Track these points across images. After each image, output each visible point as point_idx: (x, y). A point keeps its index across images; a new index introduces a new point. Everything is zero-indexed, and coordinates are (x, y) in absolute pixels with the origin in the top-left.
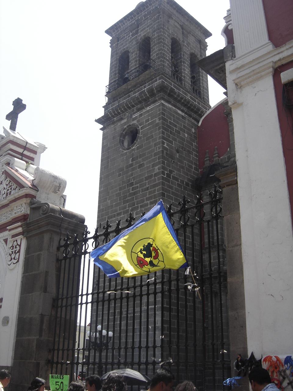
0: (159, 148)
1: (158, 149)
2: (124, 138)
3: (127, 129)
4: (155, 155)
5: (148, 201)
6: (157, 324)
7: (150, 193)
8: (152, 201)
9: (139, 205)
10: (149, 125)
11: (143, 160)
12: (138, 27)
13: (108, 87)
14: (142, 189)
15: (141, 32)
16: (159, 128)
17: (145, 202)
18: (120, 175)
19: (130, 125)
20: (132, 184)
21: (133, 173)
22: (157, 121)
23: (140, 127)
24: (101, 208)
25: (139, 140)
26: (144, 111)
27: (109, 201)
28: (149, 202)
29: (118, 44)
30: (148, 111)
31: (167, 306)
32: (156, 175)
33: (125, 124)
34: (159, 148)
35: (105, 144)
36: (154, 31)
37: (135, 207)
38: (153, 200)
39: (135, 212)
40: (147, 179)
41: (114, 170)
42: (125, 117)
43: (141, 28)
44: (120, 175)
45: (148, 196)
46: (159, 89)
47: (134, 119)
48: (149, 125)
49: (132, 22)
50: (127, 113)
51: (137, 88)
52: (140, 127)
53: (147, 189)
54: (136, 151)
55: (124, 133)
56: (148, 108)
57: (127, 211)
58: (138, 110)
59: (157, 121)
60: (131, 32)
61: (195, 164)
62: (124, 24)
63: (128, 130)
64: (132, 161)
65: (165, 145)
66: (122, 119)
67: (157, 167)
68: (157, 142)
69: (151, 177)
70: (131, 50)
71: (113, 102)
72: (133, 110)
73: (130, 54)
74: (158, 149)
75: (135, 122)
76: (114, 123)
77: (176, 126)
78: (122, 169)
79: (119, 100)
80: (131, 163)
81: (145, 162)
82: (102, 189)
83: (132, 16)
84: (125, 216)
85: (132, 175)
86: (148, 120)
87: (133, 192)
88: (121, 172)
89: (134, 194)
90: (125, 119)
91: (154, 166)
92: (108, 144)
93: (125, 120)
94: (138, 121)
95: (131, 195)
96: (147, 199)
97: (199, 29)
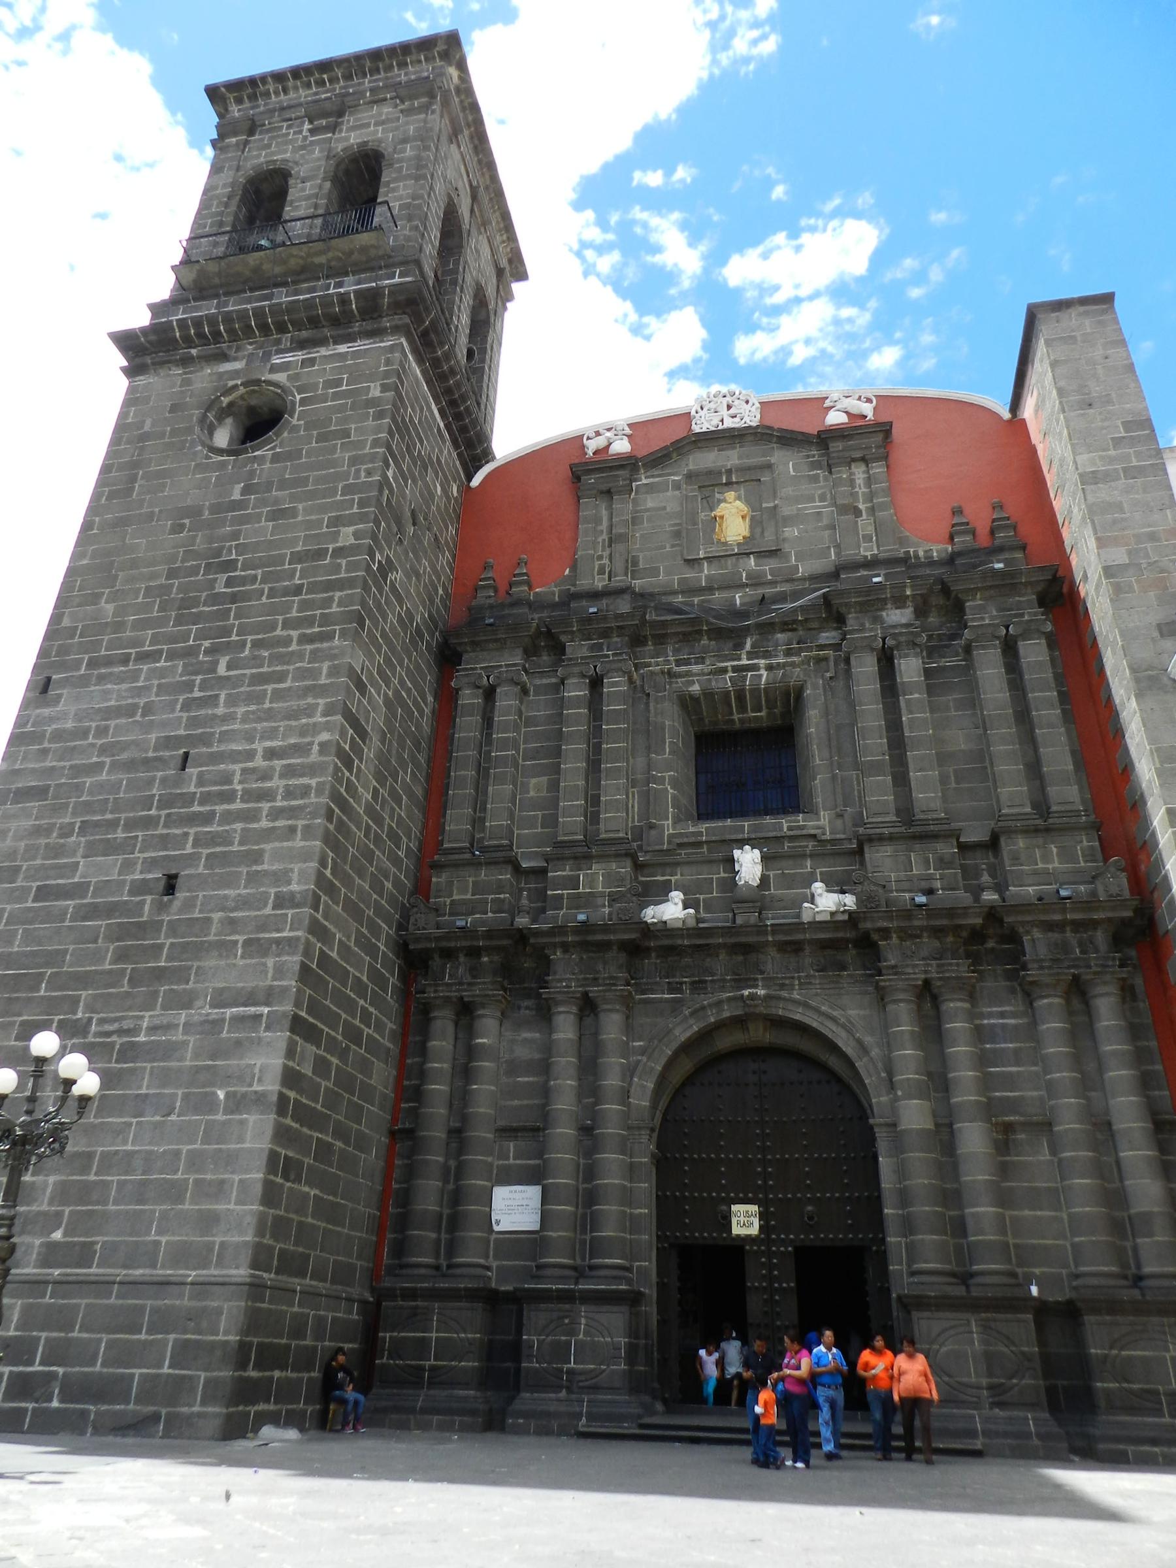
0: (369, 473)
1: (363, 474)
2: (220, 419)
3: (242, 390)
4: (347, 490)
5: (294, 629)
6: (260, 1080)
7: (304, 606)
8: (309, 631)
9: (250, 638)
10: (336, 396)
11: (294, 498)
12: (341, 114)
13: (184, 244)
14: (271, 589)
15: (348, 130)
16: (380, 415)
17: (279, 632)
18: (178, 528)
19: (258, 382)
20: (230, 565)
21: (240, 531)
22: (375, 392)
23: (298, 397)
24: (66, 622)
25: (285, 434)
26: (324, 351)
27: (110, 608)
28: (295, 634)
29: (246, 143)
30: (343, 356)
31: (306, 1016)
32: (339, 552)
33: (235, 374)
34: (369, 473)
35: (130, 420)
36: (405, 141)
37: (229, 643)
38: (317, 630)
39: (228, 658)
40: (297, 558)
41: (157, 510)
42: (240, 354)
43: (349, 120)
44: (178, 528)
45: (294, 614)
46: (401, 298)
47: (274, 369)
48: (336, 396)
49: (316, 94)
50: (251, 344)
51: (306, 281)
52: (298, 397)
53: (298, 590)
54: (268, 465)
55: (225, 400)
56: (342, 348)
57: (191, 652)
58: (301, 345)
59: (375, 392)
60: (311, 122)
61: (445, 589)
62: (285, 91)
63: (242, 397)
64: (246, 490)
65: (390, 474)
66: (224, 357)
67: (351, 529)
68: (365, 455)
69: (320, 554)
70: (302, 171)
71: (195, 300)
72: (278, 342)
73: (291, 182)
74: (363, 474)
75: (281, 377)
76: (186, 361)
77: (422, 443)
78: (194, 512)
79: (223, 299)
80: (236, 495)
81: (300, 506)
82: (85, 562)
83: (325, 76)
84: (174, 666)
85: (235, 536)
86: (338, 382)
87: (229, 590)
88: (187, 521)
89: (234, 598)
90: (235, 359)
91: (336, 522)
92: (144, 421)
93: (238, 365)
94: (289, 378)
95: (215, 599)
96: (287, 625)
97: (505, 237)
